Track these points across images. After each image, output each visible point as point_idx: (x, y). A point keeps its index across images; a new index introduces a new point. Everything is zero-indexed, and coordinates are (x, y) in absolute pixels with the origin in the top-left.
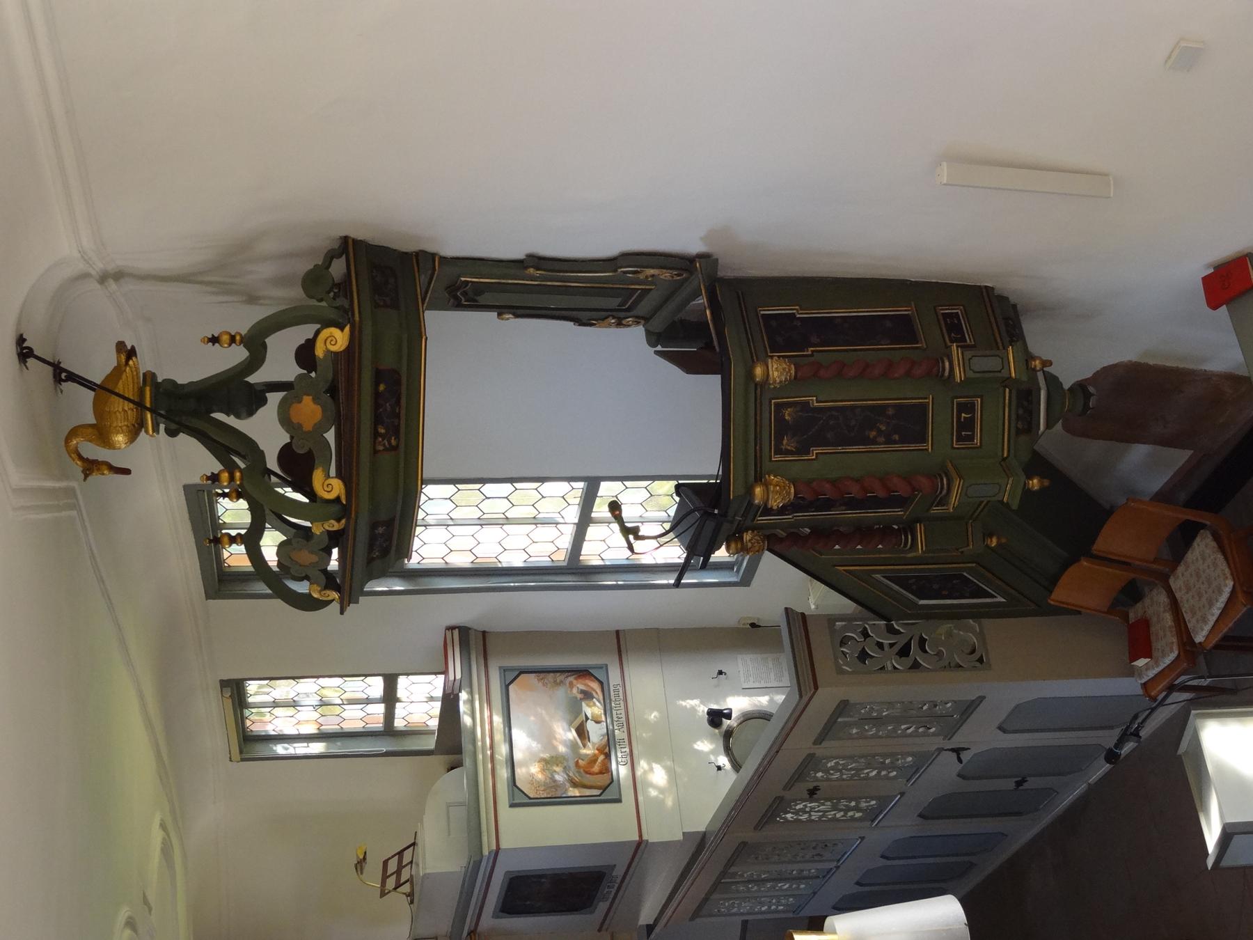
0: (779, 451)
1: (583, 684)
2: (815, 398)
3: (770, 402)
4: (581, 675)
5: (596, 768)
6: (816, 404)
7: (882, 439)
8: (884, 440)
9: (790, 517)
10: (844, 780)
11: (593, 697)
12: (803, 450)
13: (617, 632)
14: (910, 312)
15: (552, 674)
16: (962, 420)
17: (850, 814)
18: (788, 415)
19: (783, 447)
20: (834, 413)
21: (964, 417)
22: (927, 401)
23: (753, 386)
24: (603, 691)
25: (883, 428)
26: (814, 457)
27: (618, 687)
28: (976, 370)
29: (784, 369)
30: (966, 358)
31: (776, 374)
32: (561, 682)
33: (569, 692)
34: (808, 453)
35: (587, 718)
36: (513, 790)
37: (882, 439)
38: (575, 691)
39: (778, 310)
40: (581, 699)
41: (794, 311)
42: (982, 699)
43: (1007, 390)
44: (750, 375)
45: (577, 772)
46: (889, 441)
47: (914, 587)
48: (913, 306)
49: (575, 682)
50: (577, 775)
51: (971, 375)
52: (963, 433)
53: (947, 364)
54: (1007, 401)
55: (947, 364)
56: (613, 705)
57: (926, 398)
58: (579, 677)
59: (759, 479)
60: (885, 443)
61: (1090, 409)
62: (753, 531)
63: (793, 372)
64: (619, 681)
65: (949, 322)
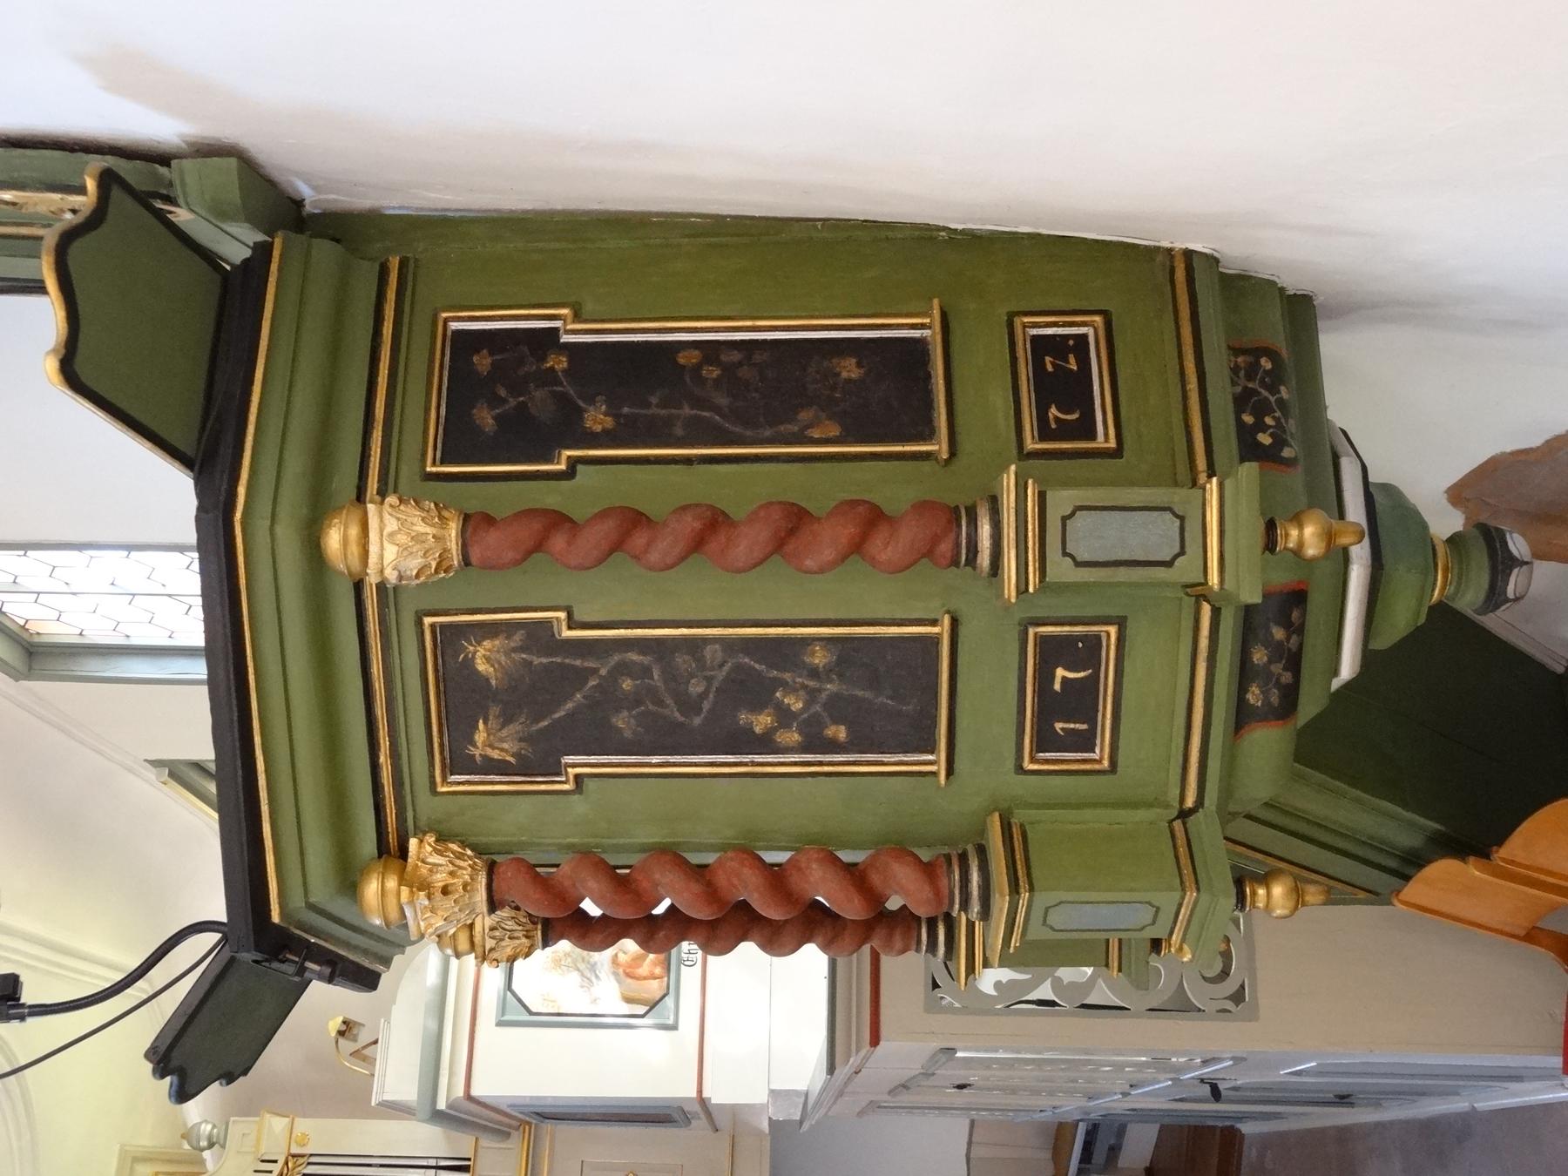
0: (459, 762)
2: (562, 615)
3: (420, 623)
6: (568, 634)
7: (794, 737)
8: (796, 737)
14: (927, 333)
16: (1057, 687)
18: (485, 658)
19: (477, 753)
20: (634, 657)
21: (1064, 679)
22: (936, 630)
25: (797, 705)
28: (1083, 556)
29: (418, 538)
31: (391, 552)
34: (556, 770)
36: (505, 995)
37: (794, 737)
39: (502, 318)
41: (557, 324)
46: (815, 742)
48: (936, 313)
51: (1061, 570)
52: (1059, 726)
53: (985, 530)
54: (1204, 643)
55: (985, 530)
57: (934, 623)
59: (392, 851)
63: (453, 545)
65: (1050, 368)
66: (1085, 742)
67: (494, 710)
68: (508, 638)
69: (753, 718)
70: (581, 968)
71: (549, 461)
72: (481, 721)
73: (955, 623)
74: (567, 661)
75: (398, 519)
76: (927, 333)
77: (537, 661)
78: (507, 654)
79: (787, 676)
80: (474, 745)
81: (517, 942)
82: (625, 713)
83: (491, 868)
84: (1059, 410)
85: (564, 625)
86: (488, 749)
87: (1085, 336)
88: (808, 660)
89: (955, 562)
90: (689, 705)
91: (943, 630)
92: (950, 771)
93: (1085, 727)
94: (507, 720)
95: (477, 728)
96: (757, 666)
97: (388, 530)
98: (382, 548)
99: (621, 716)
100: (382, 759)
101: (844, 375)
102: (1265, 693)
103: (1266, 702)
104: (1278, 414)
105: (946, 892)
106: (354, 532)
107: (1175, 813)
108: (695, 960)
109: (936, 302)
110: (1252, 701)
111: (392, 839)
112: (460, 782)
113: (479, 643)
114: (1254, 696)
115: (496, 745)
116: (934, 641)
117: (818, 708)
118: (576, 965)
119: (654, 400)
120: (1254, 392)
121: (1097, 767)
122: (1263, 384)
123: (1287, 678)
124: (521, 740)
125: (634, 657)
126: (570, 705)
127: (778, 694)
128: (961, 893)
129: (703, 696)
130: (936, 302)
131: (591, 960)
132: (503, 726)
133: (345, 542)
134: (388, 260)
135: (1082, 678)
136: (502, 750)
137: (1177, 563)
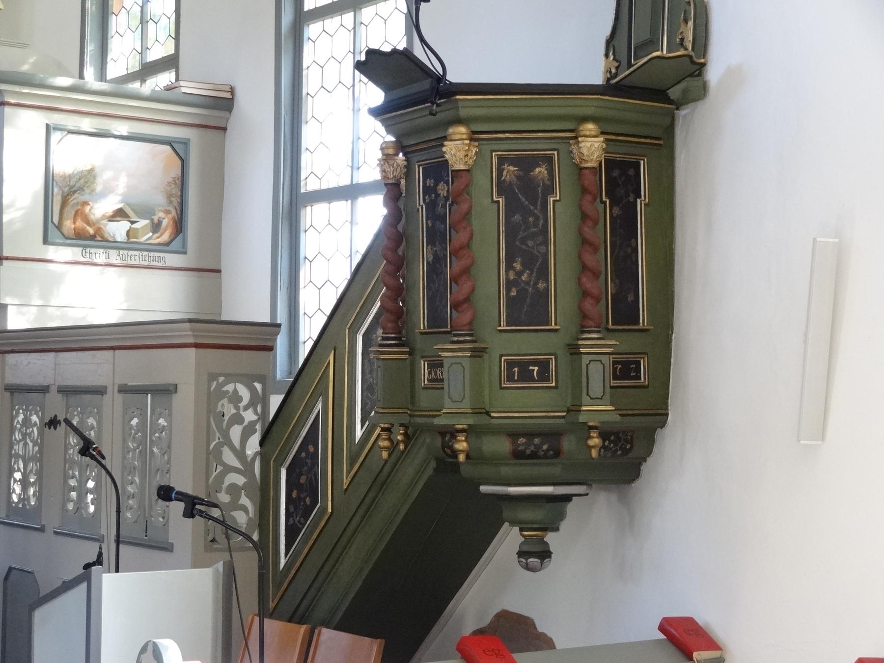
0: (502, 160)
1: (168, 223)
2: (558, 198)
3: (554, 150)
4: (176, 225)
6: (552, 199)
7: (512, 276)
8: (512, 278)
9: (422, 203)
10: (66, 451)
11: (154, 232)
12: (503, 188)
13: (219, 271)
14: (641, 325)
15: (179, 193)
16: (531, 368)
18: (540, 171)
19: (505, 166)
20: (541, 222)
22: (553, 324)
23: (570, 126)
24: (159, 244)
26: (495, 199)
27: (164, 263)
28: (591, 367)
30: (605, 359)
32: (171, 202)
34: (499, 194)
35: (133, 223)
37: (512, 276)
38: (161, 215)
40: (152, 220)
43: (565, 414)
44: (585, 119)
45: (78, 203)
46: (509, 284)
47: (303, 455)
48: (648, 328)
49: (170, 216)
50: (75, 201)
51: (585, 360)
52: (516, 369)
54: (552, 414)
56: (145, 253)
57: (556, 324)
58: (175, 222)
59: (473, 137)
60: (508, 281)
61: (527, 561)
62: (406, 167)
63: (589, 165)
64: (168, 264)
65: (631, 366)
66: (510, 378)
67: (521, 173)
68: (548, 180)
69: (519, 262)
70: (81, 181)
71: (606, 195)
72: (517, 169)
73: (556, 330)
74: (540, 199)
75: (598, 147)
76: (641, 325)
77: (540, 189)
78: (541, 179)
79: (535, 274)
80: (508, 166)
81: (392, 173)
82: (520, 218)
83: (468, 171)
84: (620, 368)
85: (554, 199)
86: (507, 171)
87: (640, 379)
88: (541, 281)
89: (583, 327)
90: (524, 241)
91: (553, 327)
92: (501, 331)
93: (516, 378)
94: (518, 177)
95: (515, 167)
96: (538, 264)
97: (595, 144)
98: (589, 142)
99: (520, 217)
100: (507, 135)
101: (629, 296)
102: (523, 444)
103: (519, 445)
104: (613, 449)
105: (462, 328)
106: (593, 133)
107: (487, 410)
108: (86, 257)
109: (652, 327)
110: (520, 440)
111: (476, 136)
112: (495, 161)
113: (546, 169)
114: (522, 440)
115: (508, 174)
116: (548, 323)
117: (523, 285)
118: (83, 177)
119: (621, 230)
120: (620, 441)
121: (503, 383)
122: (623, 444)
123: (528, 452)
124: (510, 182)
125: (541, 222)
126: (523, 199)
127: (528, 271)
128: (465, 334)
129: (527, 245)
130: (652, 327)
131: (86, 188)
132: (515, 176)
133: (590, 130)
134: (662, 140)
135: (534, 376)
136: (507, 175)
137: (588, 397)
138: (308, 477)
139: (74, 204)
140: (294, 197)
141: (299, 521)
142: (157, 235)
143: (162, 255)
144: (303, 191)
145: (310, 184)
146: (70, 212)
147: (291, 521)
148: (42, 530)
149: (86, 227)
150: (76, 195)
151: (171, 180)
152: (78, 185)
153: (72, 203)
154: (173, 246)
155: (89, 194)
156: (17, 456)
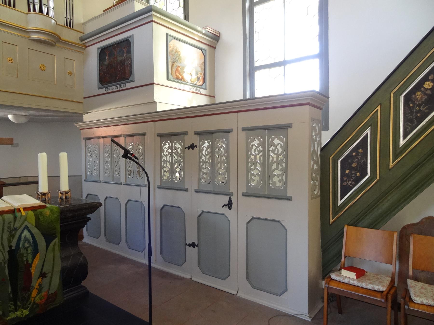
5: (178, 74)
15: (204, 68)
17: (167, 174)
24: (199, 85)
27: (200, 92)
32: (202, 71)
33: (199, 72)
38: (200, 75)
40: (197, 76)
42: (289, 199)
49: (202, 76)
50: (175, 65)
56: (196, 88)
64: (202, 93)
138: (358, 164)
139: (175, 66)
140: (251, 69)
141: (351, 184)
142: (199, 82)
143: (200, 89)
144: (255, 66)
145: (257, 64)
146: (174, 70)
147: (345, 184)
148: (186, 190)
149: (179, 76)
150: (176, 63)
151: (202, 63)
152: (176, 59)
153: (175, 65)
154: (204, 86)
155: (180, 63)
156: (166, 161)
